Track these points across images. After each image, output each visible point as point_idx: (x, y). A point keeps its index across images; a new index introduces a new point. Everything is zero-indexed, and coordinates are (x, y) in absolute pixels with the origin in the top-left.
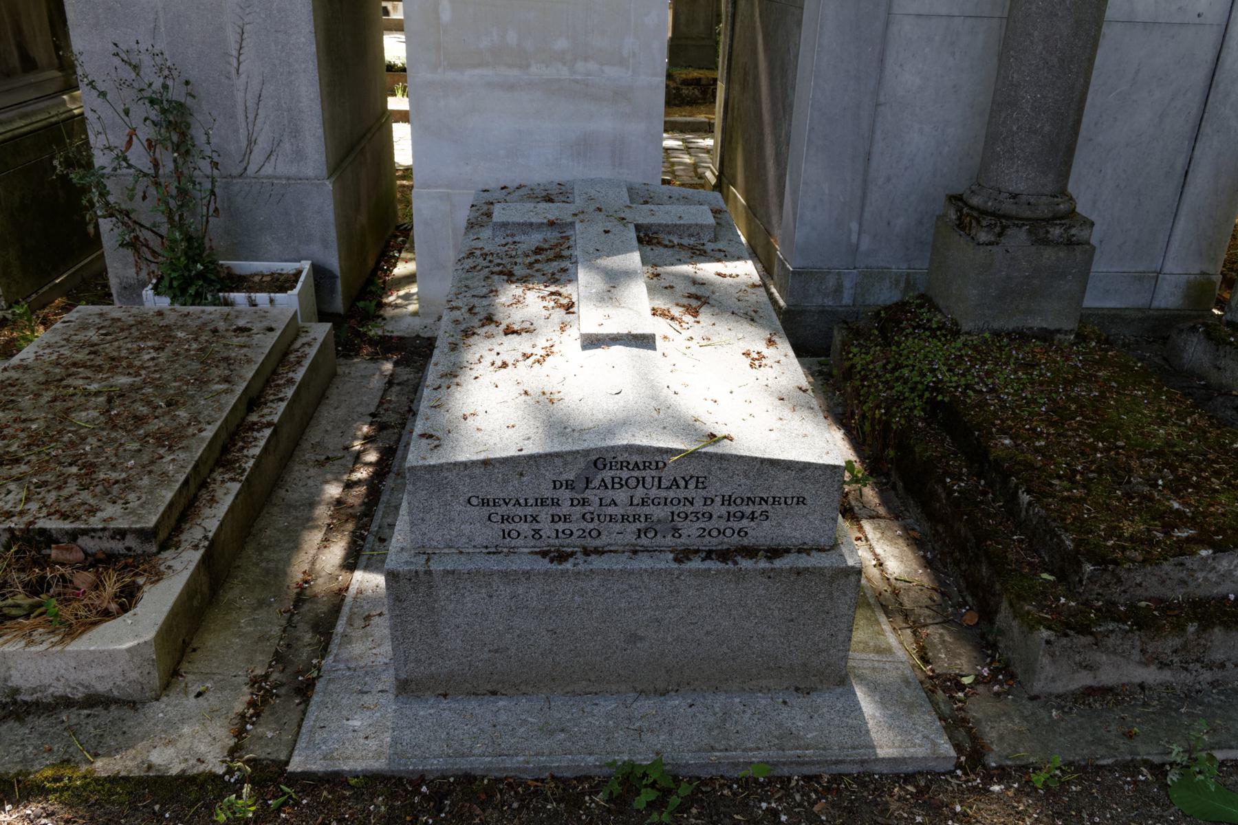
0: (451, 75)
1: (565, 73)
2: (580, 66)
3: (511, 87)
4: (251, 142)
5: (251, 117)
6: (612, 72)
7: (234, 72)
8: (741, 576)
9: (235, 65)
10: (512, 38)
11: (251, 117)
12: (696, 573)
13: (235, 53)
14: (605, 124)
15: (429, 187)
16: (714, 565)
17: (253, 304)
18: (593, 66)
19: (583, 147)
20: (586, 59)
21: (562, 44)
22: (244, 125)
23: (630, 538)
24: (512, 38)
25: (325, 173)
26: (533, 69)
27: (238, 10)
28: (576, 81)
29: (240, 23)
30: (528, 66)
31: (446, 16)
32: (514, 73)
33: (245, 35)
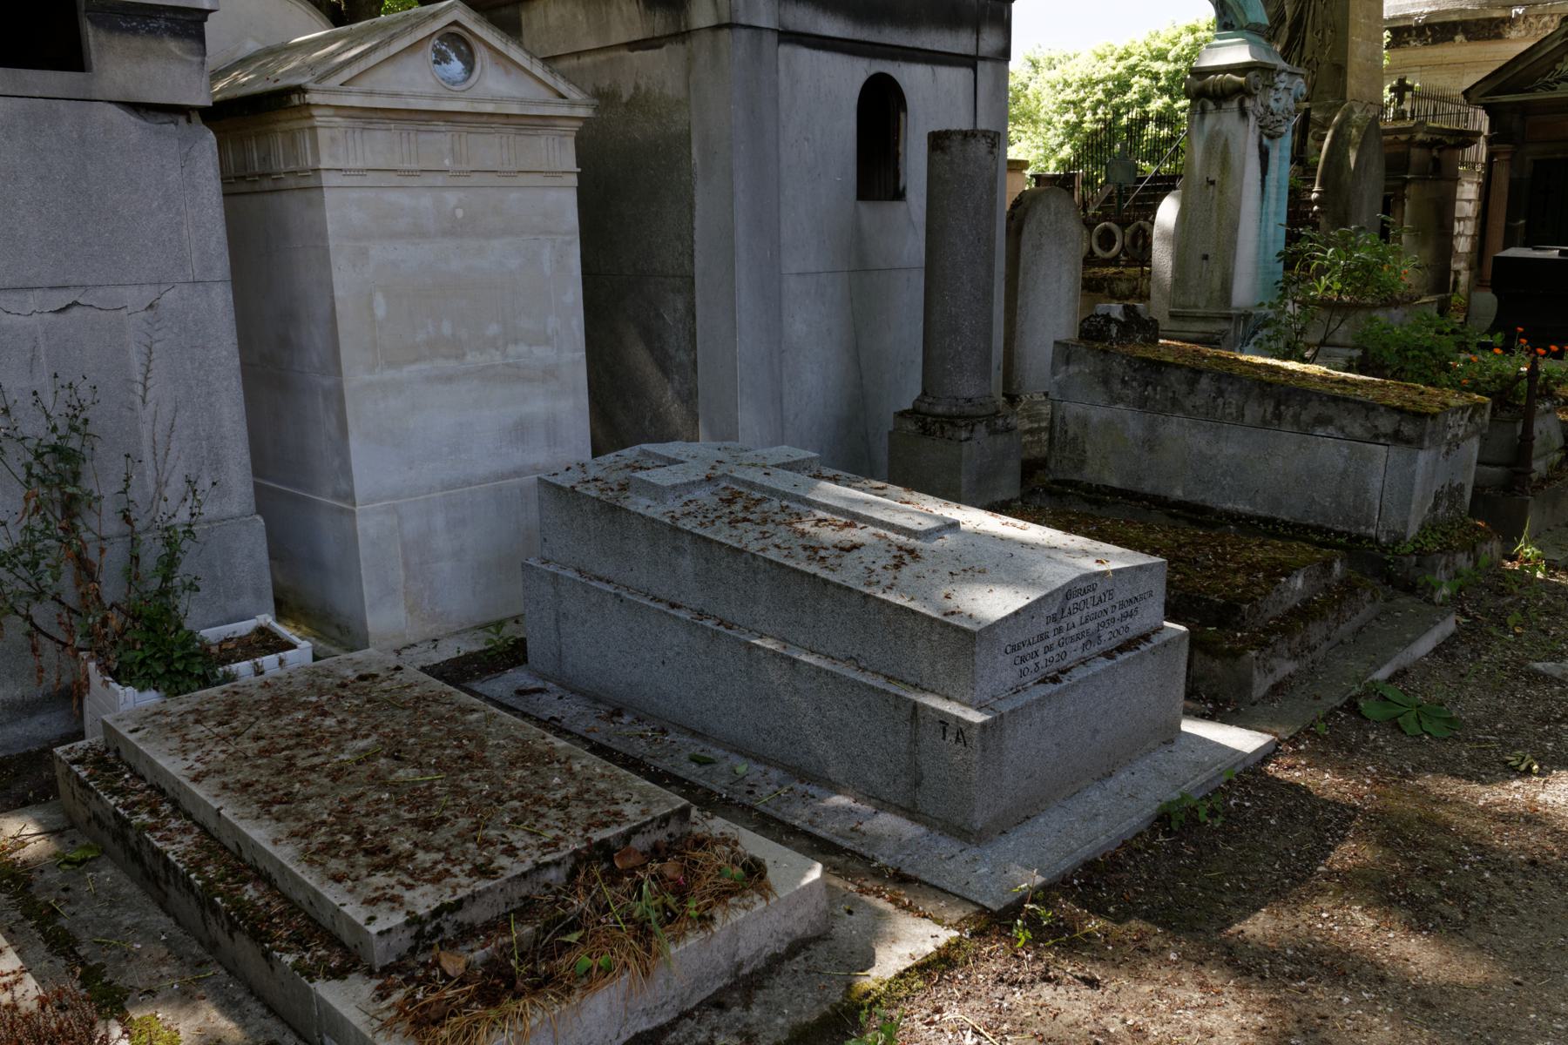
0: (389, 374)
1: (498, 359)
2: (511, 349)
3: (449, 379)
4: (160, 484)
5: (161, 453)
6: (539, 351)
7: (139, 401)
8: (1142, 657)
9: (140, 392)
10: (446, 328)
11: (161, 453)
12: (1126, 663)
13: (139, 378)
14: (537, 405)
15: (373, 501)
16: (1127, 655)
17: (259, 672)
18: (523, 348)
19: (520, 431)
20: (516, 342)
21: (493, 329)
22: (151, 464)
23: (1079, 654)
24: (446, 328)
25: (253, 508)
26: (469, 358)
27: (145, 326)
28: (508, 365)
29: (148, 342)
30: (464, 355)
31: (380, 312)
32: (451, 365)
33: (154, 356)
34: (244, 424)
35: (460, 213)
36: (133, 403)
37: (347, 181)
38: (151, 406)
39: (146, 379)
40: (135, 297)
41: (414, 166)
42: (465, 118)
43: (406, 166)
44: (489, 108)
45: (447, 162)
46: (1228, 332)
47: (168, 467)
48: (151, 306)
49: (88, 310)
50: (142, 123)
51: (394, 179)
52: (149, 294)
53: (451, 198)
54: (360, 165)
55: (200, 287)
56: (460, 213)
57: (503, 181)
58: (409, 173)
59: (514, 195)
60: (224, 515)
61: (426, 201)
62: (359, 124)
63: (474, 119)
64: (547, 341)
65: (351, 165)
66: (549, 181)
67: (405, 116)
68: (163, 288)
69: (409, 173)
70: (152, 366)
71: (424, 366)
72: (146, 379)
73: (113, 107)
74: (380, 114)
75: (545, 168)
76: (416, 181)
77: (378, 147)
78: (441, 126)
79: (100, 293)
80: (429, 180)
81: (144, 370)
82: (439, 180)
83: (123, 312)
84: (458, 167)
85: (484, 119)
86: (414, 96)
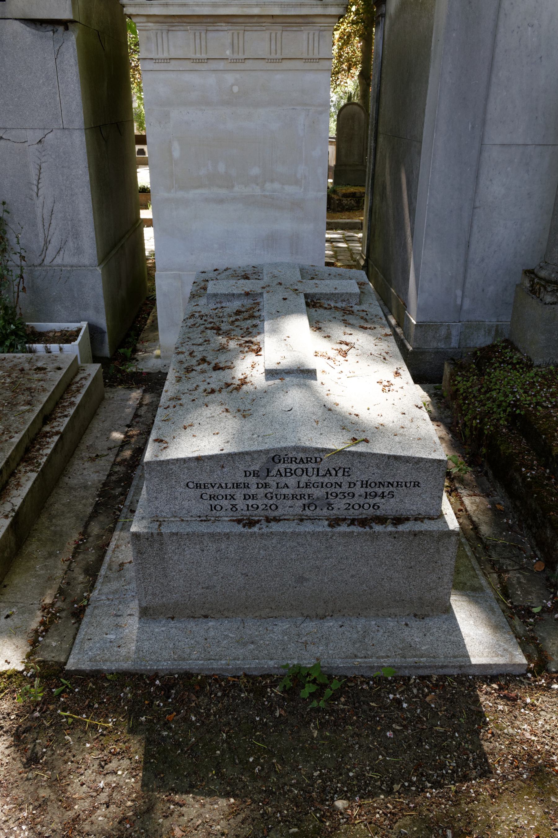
0: (180, 194)
1: (257, 190)
2: (268, 186)
3: (221, 201)
4: (47, 242)
5: (47, 225)
6: (290, 189)
7: (35, 195)
8: (375, 536)
9: (36, 190)
10: (222, 168)
11: (47, 225)
12: (344, 535)
13: (35, 182)
14: (286, 225)
15: (166, 270)
16: (356, 529)
17: (48, 351)
18: (277, 186)
19: (271, 241)
20: (272, 181)
21: (255, 171)
22: (42, 231)
23: (299, 511)
24: (222, 168)
25: (96, 262)
26: (236, 189)
27: (37, 153)
28: (265, 196)
29: (39, 162)
30: (233, 186)
31: (176, 154)
32: (223, 192)
33: (42, 170)
34: (92, 214)
35: (236, 89)
36: (32, 196)
37: (157, 66)
38: (41, 198)
39: (38, 183)
40: (33, 136)
41: (204, 56)
42: (240, 20)
43: (198, 56)
44: (256, 11)
45: (228, 52)
46: (362, 195)
47: (50, 233)
48: (40, 141)
49: (8, 142)
50: (34, 31)
51: (188, 65)
52: (39, 135)
53: (230, 78)
54: (166, 55)
55: (67, 132)
56: (236, 89)
57: (271, 66)
58: (200, 61)
59: (278, 76)
60: (80, 264)
61: (211, 80)
62: (165, 27)
63: (247, 20)
64: (297, 182)
65: (160, 56)
66: (308, 66)
67: (196, 20)
68: (46, 132)
69: (200, 61)
70: (41, 176)
71: (205, 191)
72: (38, 183)
73: (17, 22)
74: (178, 20)
75: (305, 56)
76: (204, 67)
77: (180, 42)
78: (224, 26)
79: (13, 132)
80: (213, 65)
81: (37, 178)
82: (221, 65)
83: (26, 144)
84: (236, 56)
85: (255, 20)
86: (197, 5)
